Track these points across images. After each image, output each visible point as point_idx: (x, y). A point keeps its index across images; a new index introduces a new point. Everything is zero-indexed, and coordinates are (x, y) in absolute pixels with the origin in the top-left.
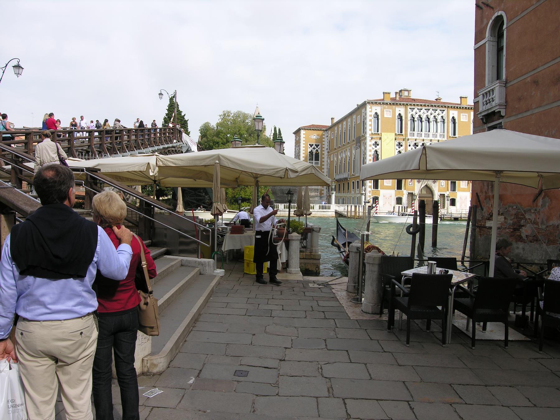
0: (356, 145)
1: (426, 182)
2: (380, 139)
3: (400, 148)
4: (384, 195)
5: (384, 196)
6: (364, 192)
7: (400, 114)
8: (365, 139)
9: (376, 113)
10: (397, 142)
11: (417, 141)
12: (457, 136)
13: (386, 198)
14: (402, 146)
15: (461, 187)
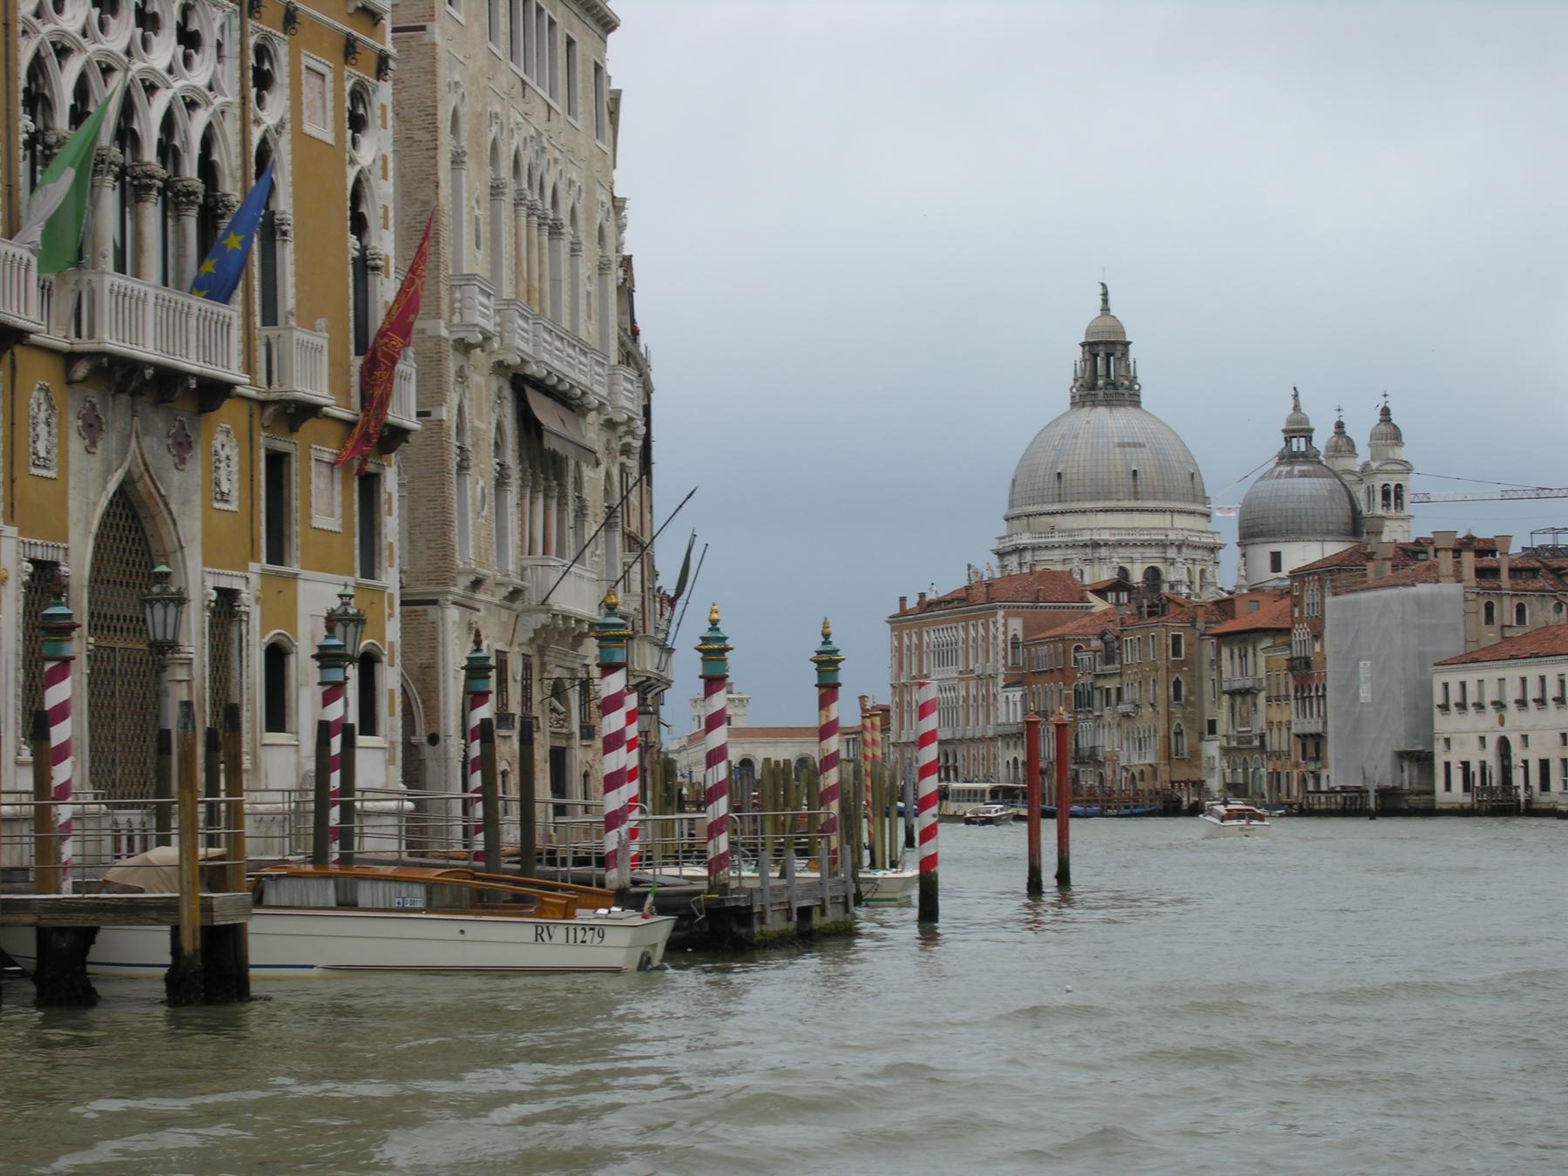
1: (134, 444)
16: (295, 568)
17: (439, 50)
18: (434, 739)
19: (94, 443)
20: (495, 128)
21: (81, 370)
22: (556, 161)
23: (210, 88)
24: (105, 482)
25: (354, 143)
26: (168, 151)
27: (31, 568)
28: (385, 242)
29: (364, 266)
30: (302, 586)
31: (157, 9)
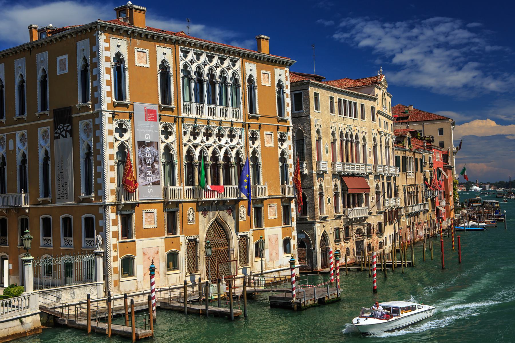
0: (56, 128)
1: (217, 212)
2: (131, 116)
3: (167, 138)
4: (145, 250)
5: (144, 254)
6: (100, 250)
7: (164, 62)
8: (99, 114)
9: (118, 55)
10: (162, 124)
11: (199, 123)
12: (258, 113)
13: (149, 258)
14: (170, 133)
15: (270, 217)
16: (263, 228)
17: (311, 120)
18: (314, 249)
19: (205, 215)
20: (333, 129)
21: (200, 204)
22: (357, 129)
23: (238, 144)
24: (209, 221)
25: (282, 145)
26: (227, 158)
27: (188, 241)
28: (290, 162)
29: (284, 168)
30: (265, 230)
31: (222, 133)
